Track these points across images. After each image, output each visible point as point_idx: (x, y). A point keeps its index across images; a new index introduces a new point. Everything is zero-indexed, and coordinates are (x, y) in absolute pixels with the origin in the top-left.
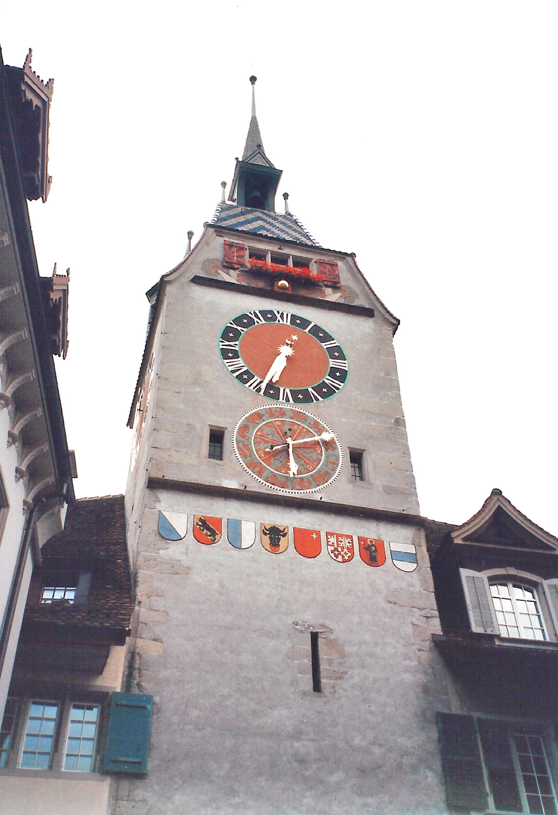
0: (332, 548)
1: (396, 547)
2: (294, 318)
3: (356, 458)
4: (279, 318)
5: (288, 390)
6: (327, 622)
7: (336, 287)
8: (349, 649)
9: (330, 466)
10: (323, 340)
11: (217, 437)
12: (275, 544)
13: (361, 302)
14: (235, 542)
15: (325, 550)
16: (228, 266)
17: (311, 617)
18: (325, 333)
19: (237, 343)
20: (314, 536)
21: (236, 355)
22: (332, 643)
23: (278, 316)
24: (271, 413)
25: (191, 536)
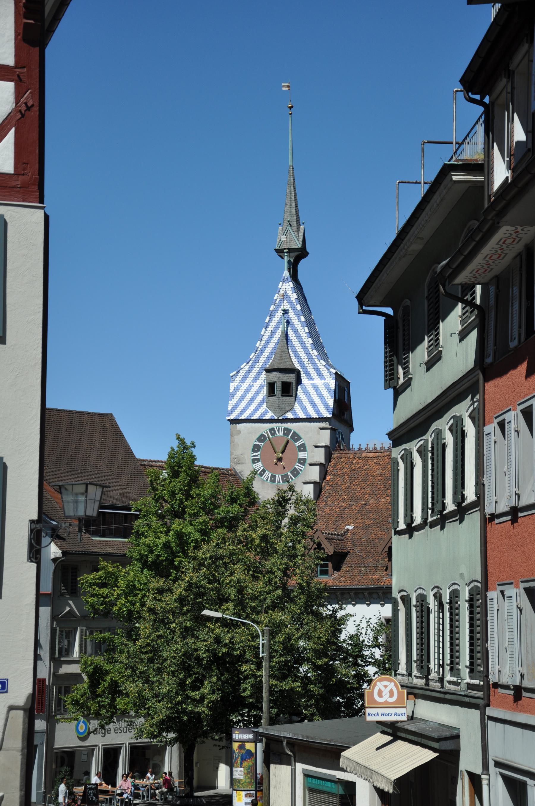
2: (285, 429)
4: (277, 432)
5: (280, 476)
10: (296, 441)
19: (259, 453)
21: (258, 460)
23: (276, 430)
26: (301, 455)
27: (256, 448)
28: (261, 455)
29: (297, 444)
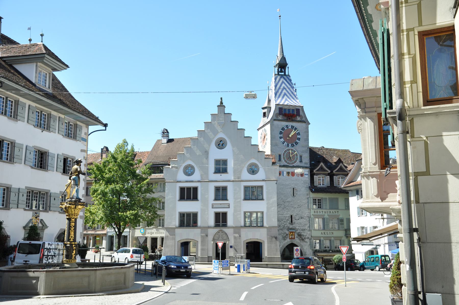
1: (306, 173)
7: (299, 115)
12: (288, 175)
13: (304, 119)
15: (295, 175)
17: (293, 186)
22: (296, 189)
26: (298, 136)
27: (281, 133)
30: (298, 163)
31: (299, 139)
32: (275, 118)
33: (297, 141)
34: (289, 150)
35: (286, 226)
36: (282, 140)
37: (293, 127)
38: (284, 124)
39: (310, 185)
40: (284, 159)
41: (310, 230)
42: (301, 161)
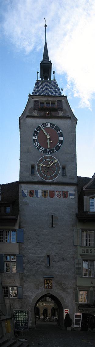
0: (56, 195)
1: (71, 192)
3: (64, 168)
6: (55, 213)
8: (58, 218)
9: (58, 172)
11: (33, 167)
12: (45, 195)
14: (37, 196)
15: (55, 195)
16: (35, 109)
18: (58, 128)
20: (53, 192)
23: (47, 125)
24: (45, 158)
25: (28, 196)
26: (60, 138)
27: (35, 134)
28: (38, 137)
29: (58, 132)
30: (59, 178)
31: (61, 142)
32: (27, 114)
33: (59, 145)
34: (47, 158)
35: (40, 270)
36: (37, 144)
37: (52, 125)
38: (40, 121)
39: (77, 211)
40: (39, 171)
41: (76, 278)
42: (64, 175)
